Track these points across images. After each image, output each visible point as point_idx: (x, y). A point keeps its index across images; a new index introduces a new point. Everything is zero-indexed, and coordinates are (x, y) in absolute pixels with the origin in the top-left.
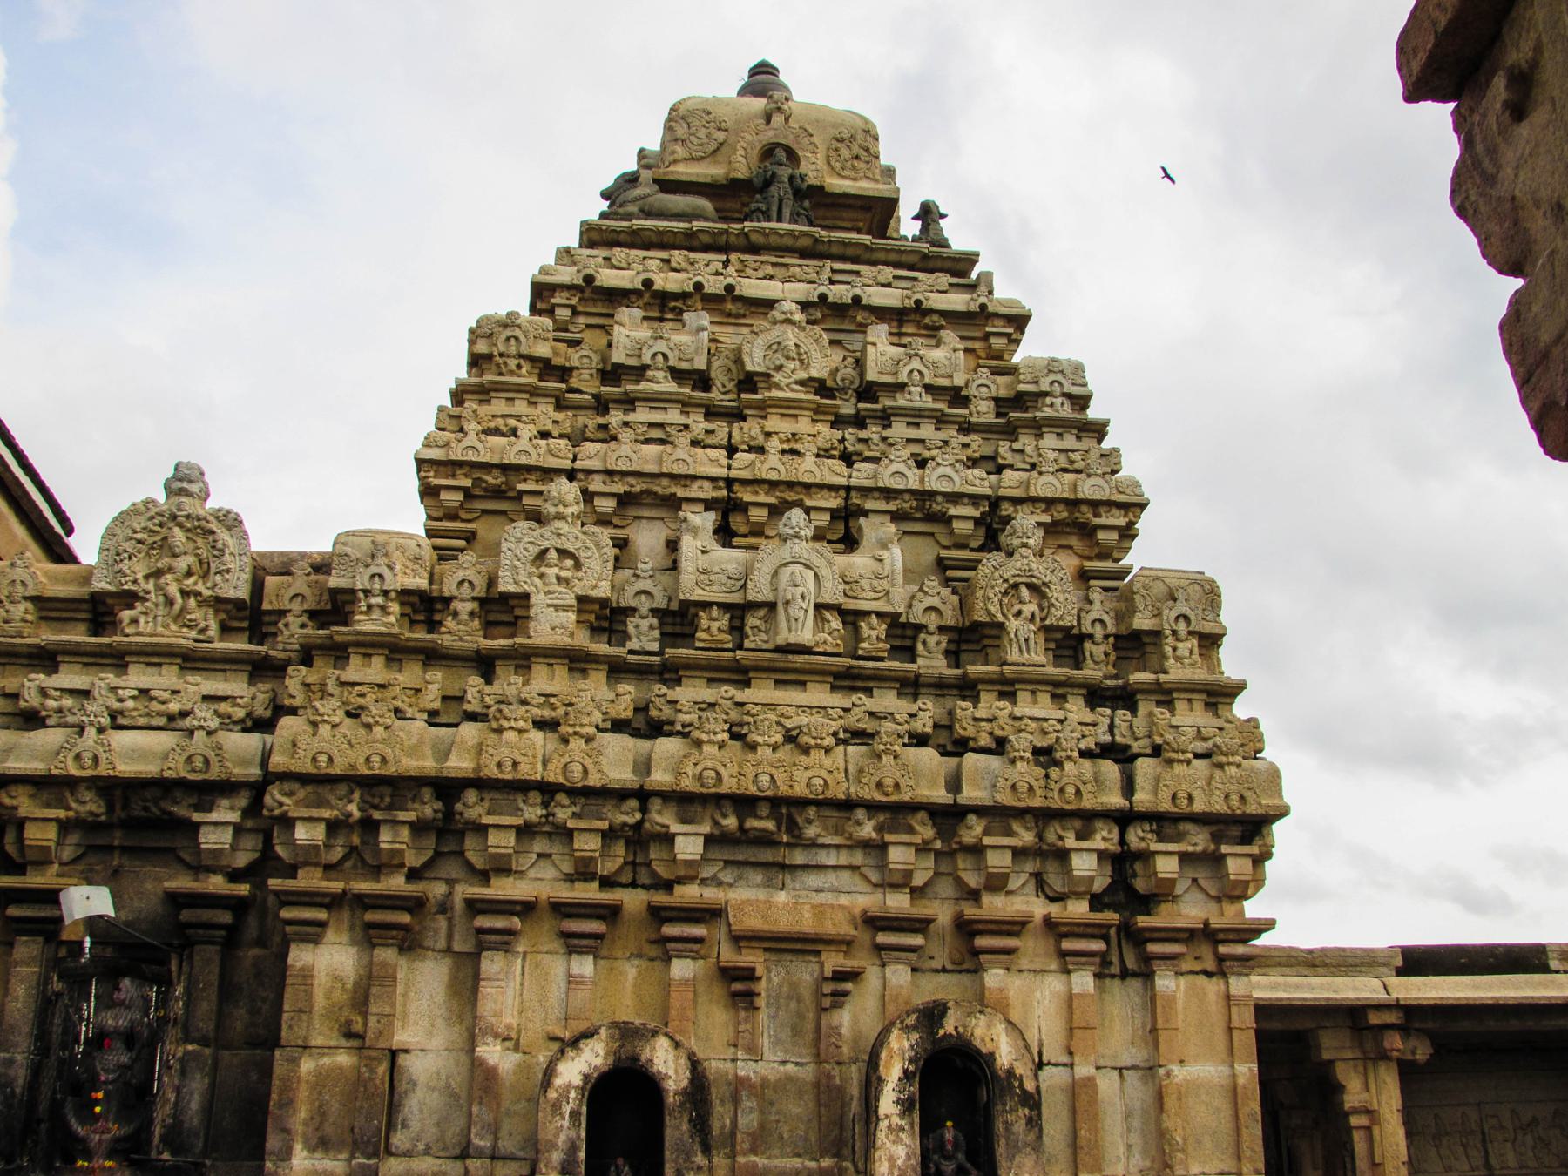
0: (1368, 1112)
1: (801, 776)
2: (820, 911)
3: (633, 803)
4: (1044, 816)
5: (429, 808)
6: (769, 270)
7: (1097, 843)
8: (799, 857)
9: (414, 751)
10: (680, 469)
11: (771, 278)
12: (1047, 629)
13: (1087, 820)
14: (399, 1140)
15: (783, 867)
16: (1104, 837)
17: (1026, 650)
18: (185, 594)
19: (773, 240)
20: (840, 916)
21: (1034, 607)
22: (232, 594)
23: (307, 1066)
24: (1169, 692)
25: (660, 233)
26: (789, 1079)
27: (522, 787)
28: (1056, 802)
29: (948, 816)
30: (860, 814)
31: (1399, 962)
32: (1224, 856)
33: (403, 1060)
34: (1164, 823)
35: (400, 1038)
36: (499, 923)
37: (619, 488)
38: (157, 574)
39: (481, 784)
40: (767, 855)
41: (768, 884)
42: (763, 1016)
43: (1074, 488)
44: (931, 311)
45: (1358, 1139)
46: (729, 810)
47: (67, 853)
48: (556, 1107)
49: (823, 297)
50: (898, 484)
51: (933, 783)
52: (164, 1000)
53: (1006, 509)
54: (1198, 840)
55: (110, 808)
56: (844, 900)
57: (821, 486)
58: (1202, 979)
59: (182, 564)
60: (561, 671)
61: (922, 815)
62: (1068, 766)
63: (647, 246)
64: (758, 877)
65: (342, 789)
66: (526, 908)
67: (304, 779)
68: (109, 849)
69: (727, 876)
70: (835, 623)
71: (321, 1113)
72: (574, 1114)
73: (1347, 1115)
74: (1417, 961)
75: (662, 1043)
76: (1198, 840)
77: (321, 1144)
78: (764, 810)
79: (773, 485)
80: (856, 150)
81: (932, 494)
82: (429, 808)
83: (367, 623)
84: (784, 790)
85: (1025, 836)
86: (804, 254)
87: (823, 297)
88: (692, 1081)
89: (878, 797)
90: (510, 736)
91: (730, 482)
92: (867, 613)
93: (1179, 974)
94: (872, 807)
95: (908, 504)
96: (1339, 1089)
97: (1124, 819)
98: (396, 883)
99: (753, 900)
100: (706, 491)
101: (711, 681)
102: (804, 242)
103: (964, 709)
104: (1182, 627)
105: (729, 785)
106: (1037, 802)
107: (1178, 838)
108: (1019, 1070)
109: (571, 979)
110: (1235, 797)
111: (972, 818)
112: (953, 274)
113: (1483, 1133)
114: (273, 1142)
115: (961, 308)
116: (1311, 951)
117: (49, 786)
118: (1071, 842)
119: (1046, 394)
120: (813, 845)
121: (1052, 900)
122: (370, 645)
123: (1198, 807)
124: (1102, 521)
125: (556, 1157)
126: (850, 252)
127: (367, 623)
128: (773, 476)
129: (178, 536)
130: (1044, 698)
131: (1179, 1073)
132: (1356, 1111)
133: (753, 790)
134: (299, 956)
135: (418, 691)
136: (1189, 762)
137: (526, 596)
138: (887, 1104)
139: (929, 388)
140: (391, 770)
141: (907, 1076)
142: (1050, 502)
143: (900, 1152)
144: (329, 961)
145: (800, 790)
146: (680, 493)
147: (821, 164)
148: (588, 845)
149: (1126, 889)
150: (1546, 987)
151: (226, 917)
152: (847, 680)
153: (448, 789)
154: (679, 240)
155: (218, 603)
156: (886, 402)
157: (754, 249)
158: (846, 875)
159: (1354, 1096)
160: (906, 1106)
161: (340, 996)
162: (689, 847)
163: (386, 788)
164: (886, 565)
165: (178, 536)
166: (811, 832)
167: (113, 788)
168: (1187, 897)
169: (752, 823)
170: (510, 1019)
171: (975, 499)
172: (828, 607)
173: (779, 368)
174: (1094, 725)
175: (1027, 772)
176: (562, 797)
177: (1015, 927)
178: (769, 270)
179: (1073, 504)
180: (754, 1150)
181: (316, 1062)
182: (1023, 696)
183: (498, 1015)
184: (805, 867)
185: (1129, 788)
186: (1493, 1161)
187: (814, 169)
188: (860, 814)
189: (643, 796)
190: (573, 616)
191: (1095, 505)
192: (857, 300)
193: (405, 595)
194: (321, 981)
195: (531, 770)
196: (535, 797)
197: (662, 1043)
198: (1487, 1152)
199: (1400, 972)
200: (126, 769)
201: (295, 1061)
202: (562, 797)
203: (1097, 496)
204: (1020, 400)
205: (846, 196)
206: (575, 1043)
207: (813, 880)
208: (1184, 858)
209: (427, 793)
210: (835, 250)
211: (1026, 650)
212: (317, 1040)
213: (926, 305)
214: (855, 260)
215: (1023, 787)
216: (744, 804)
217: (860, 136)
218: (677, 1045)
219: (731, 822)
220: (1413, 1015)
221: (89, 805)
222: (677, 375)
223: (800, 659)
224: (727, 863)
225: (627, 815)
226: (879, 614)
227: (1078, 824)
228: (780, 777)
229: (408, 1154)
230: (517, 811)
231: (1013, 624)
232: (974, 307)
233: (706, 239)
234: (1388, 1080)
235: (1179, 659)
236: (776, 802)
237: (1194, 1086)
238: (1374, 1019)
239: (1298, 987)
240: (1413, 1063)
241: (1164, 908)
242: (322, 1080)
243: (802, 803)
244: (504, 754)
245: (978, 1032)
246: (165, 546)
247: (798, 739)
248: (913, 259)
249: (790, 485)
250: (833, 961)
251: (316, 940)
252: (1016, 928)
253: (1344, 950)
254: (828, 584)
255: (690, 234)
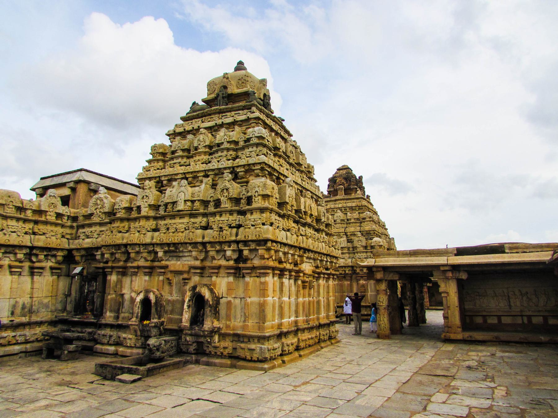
0: (447, 293)
1: (176, 238)
2: (183, 265)
3: (151, 246)
4: (221, 243)
5: (123, 249)
6: (209, 119)
7: (231, 248)
8: (181, 254)
9: (118, 239)
10: (175, 173)
11: (209, 121)
12: (231, 199)
13: (229, 243)
14: (124, 310)
15: (180, 257)
16: (234, 246)
17: (226, 205)
18: (100, 212)
19: (212, 112)
20: (187, 266)
21: (227, 194)
22: (107, 211)
23: (109, 297)
24: (252, 210)
25: (193, 116)
26: (178, 300)
27: (136, 244)
28: (221, 240)
29: (204, 244)
30: (188, 245)
31: (455, 252)
32: (258, 249)
33: (125, 296)
34: (246, 243)
35: (124, 291)
36: (133, 270)
37: (166, 178)
38: (96, 209)
39: (130, 245)
40: (175, 254)
41: (177, 260)
42: (174, 287)
43: (248, 161)
44: (238, 121)
45: (444, 299)
46: (166, 245)
47: (83, 261)
48: (136, 306)
49: (216, 124)
50: (213, 168)
51: (199, 237)
52: (96, 285)
53: (236, 169)
54: (253, 246)
55: (87, 252)
56: (189, 263)
57: (200, 171)
58: (256, 278)
59: (99, 207)
60: (144, 220)
61: (199, 244)
62: (224, 232)
63: (192, 119)
64: (175, 259)
65: (111, 247)
66: (138, 267)
67: (106, 246)
68: (88, 259)
69: (170, 259)
70: (189, 204)
71: (111, 306)
72: (138, 307)
73: (441, 293)
74: (461, 252)
75: (152, 293)
76: (253, 246)
77: (111, 311)
78: (172, 246)
79: (192, 172)
80: (243, 81)
81: (220, 169)
82: (123, 249)
83: (118, 215)
84: (174, 242)
85: (218, 248)
86: (219, 113)
87: (216, 124)
88: (156, 301)
89: (189, 241)
90: (132, 235)
91: (184, 173)
92: (195, 201)
93: (250, 277)
94: (190, 244)
95: (217, 172)
96: (439, 286)
97: (237, 242)
98: (121, 263)
99: (175, 264)
100: (180, 176)
101: (180, 218)
102: (218, 111)
103: (211, 219)
104: (256, 194)
105: (165, 241)
106: (217, 240)
107: (249, 246)
108: (210, 299)
109: (145, 281)
110: (258, 236)
111: (207, 244)
112: (248, 109)
113: (509, 296)
114: (104, 311)
115: (244, 119)
116: (430, 250)
117: (78, 250)
118: (226, 248)
119: (251, 138)
120: (182, 252)
121: (228, 260)
122: (95, 224)
123: (250, 239)
124: (256, 168)
125: (135, 315)
126: (228, 110)
127: (118, 215)
128: (191, 171)
129: (99, 202)
130: (228, 215)
131: (249, 300)
132: (443, 292)
133: (168, 242)
134: (109, 278)
135: (124, 227)
136: (249, 228)
137: (140, 206)
138: (185, 307)
139: (228, 142)
140: (115, 243)
141: (189, 301)
142: (244, 166)
143: (187, 316)
144: (113, 278)
145: (176, 241)
146: (176, 177)
147: (235, 88)
148: (145, 255)
149: (241, 259)
150: (499, 258)
151: (101, 271)
152: (192, 216)
153: (126, 245)
154: (197, 117)
155: (105, 213)
156: (222, 147)
157: (210, 115)
158: (190, 257)
159: (442, 288)
160: (189, 307)
161: (114, 285)
162: (160, 254)
163: (118, 246)
164: (203, 190)
165: (99, 202)
166: (181, 249)
167: (86, 249)
168: (255, 259)
169: (170, 248)
170: (136, 288)
171: (229, 168)
172: (188, 200)
173: (199, 144)
174: (235, 220)
175: (216, 234)
176: (141, 246)
177: (219, 267)
178: (209, 119)
179: (249, 165)
180: (171, 314)
181: (111, 297)
182: (224, 215)
183: (134, 287)
184: (182, 256)
185: (237, 235)
186: (512, 304)
187: (234, 89)
188: (188, 245)
189: (153, 245)
190: (147, 209)
191: (254, 164)
192: (222, 122)
193: (125, 208)
194: (112, 282)
195: (136, 241)
196: (138, 246)
197: (152, 293)
198: (510, 302)
199: (456, 255)
200: (86, 246)
201: (107, 296)
202: (141, 246)
203: (253, 162)
204: (248, 140)
205: (238, 93)
206: (139, 294)
207: (184, 259)
208: (251, 250)
209: (122, 247)
210: (225, 110)
211: (226, 205)
212: (111, 292)
213: (237, 120)
214: (225, 112)
215: (215, 237)
216: (168, 245)
217: (244, 77)
218: (154, 294)
219: (167, 248)
220: (455, 268)
221: (83, 252)
222: (183, 150)
223: (181, 212)
224: (170, 256)
225: (151, 248)
226: (199, 200)
227: (228, 244)
228: (173, 239)
229: (125, 313)
230: (135, 249)
231: (222, 199)
232: (246, 118)
233: (200, 115)
234: (452, 284)
235: (255, 202)
236: (174, 244)
237: (252, 303)
238: (442, 269)
239: (422, 260)
240: (462, 280)
241: (249, 262)
242: (112, 299)
243: (178, 244)
244: (131, 239)
245: (203, 291)
246: (97, 204)
247: (180, 230)
248: (241, 108)
249: (195, 172)
250: (185, 276)
251: (111, 275)
252: (193, 271)
253: (439, 249)
254: (186, 196)
255: (198, 115)
